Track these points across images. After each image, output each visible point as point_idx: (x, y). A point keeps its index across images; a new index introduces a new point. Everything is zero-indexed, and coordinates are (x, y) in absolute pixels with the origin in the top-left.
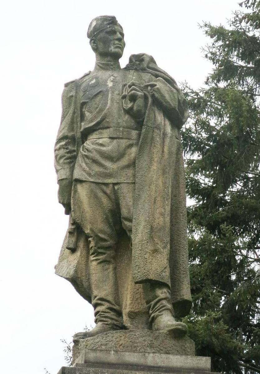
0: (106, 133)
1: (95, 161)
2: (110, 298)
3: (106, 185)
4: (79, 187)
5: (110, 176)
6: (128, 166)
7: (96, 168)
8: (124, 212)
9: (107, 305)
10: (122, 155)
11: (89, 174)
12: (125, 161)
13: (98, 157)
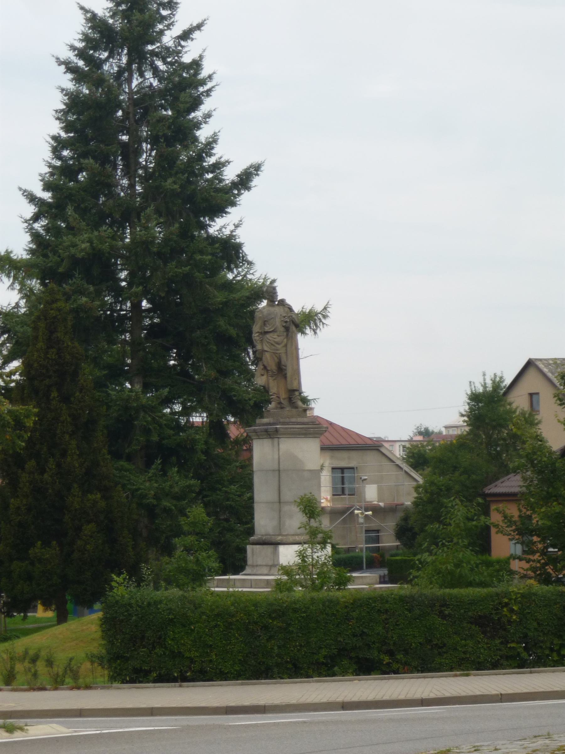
0: (276, 334)
1: (272, 344)
2: (276, 393)
3: (277, 353)
4: (266, 353)
5: (277, 350)
6: (284, 346)
7: (273, 347)
8: (283, 363)
9: (276, 395)
10: (282, 342)
11: (271, 350)
12: (283, 344)
13: (273, 343)
